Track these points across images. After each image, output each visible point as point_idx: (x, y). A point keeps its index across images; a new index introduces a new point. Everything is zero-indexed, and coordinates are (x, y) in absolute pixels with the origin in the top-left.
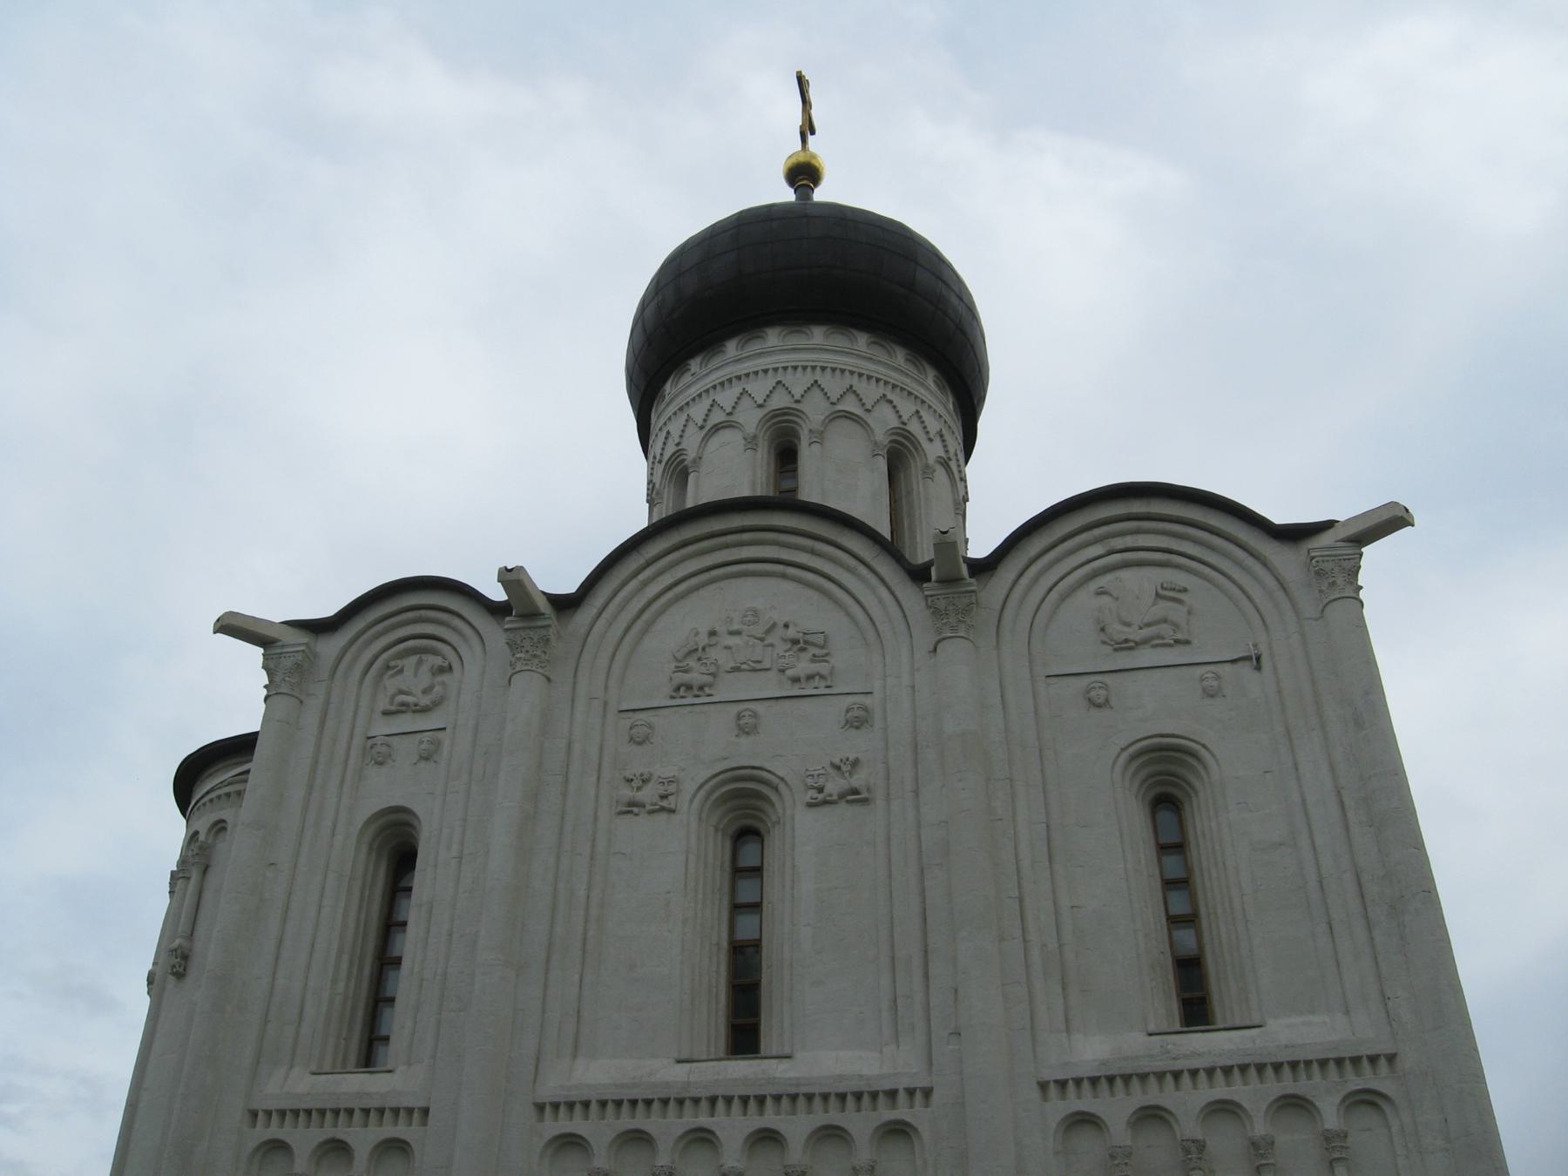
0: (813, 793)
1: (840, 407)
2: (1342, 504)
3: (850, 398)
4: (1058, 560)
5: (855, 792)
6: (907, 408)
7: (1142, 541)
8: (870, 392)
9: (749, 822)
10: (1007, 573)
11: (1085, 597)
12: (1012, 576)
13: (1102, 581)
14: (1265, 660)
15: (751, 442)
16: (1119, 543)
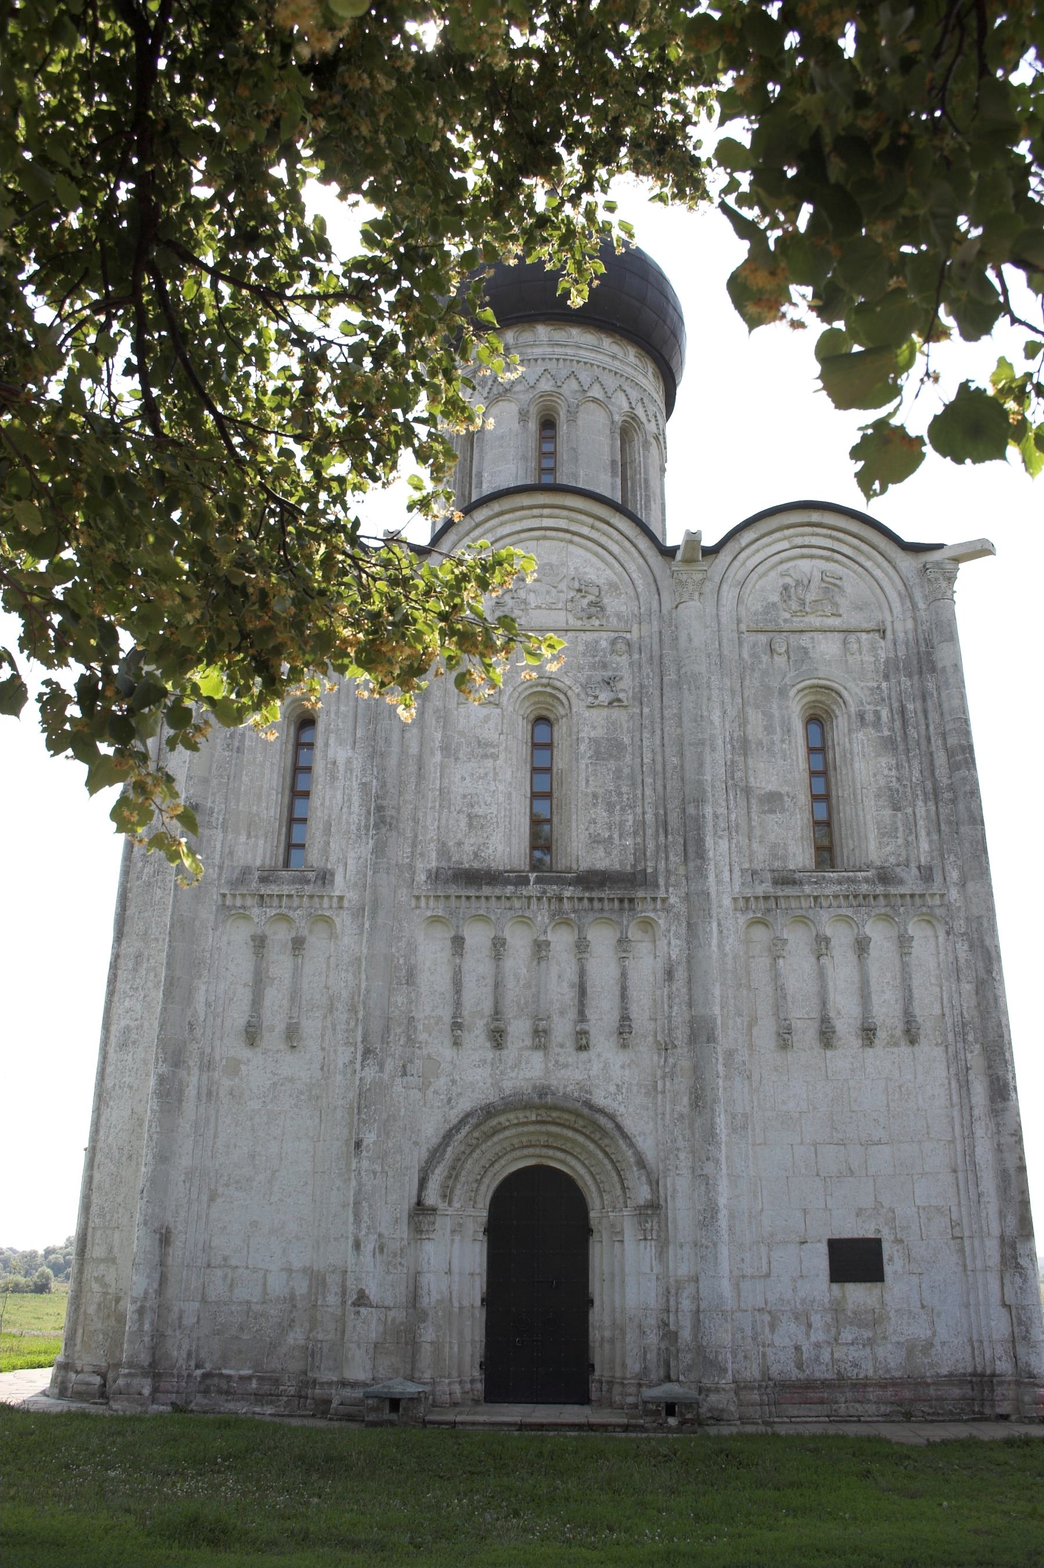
0: (590, 699)
1: (589, 394)
2: (950, 534)
3: (596, 387)
4: (758, 551)
5: (619, 700)
6: (634, 394)
7: (814, 541)
8: (611, 382)
9: (545, 713)
10: (725, 556)
11: (773, 574)
12: (729, 559)
13: (785, 566)
14: (889, 633)
15: (523, 416)
16: (799, 541)
